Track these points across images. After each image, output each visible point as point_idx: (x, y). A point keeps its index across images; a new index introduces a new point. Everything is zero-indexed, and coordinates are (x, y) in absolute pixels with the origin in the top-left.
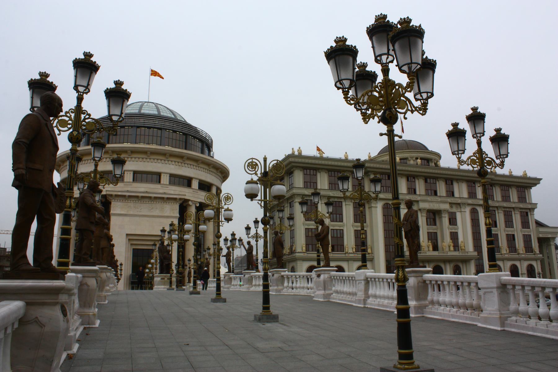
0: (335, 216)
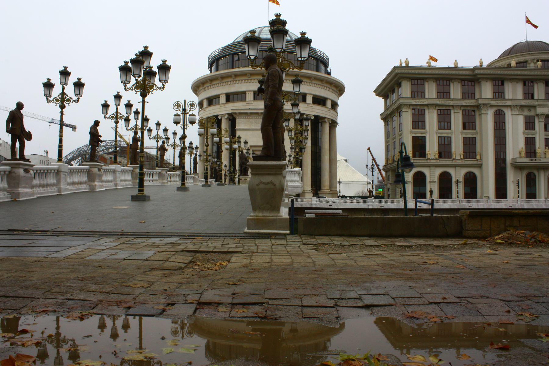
0: (442, 123)
